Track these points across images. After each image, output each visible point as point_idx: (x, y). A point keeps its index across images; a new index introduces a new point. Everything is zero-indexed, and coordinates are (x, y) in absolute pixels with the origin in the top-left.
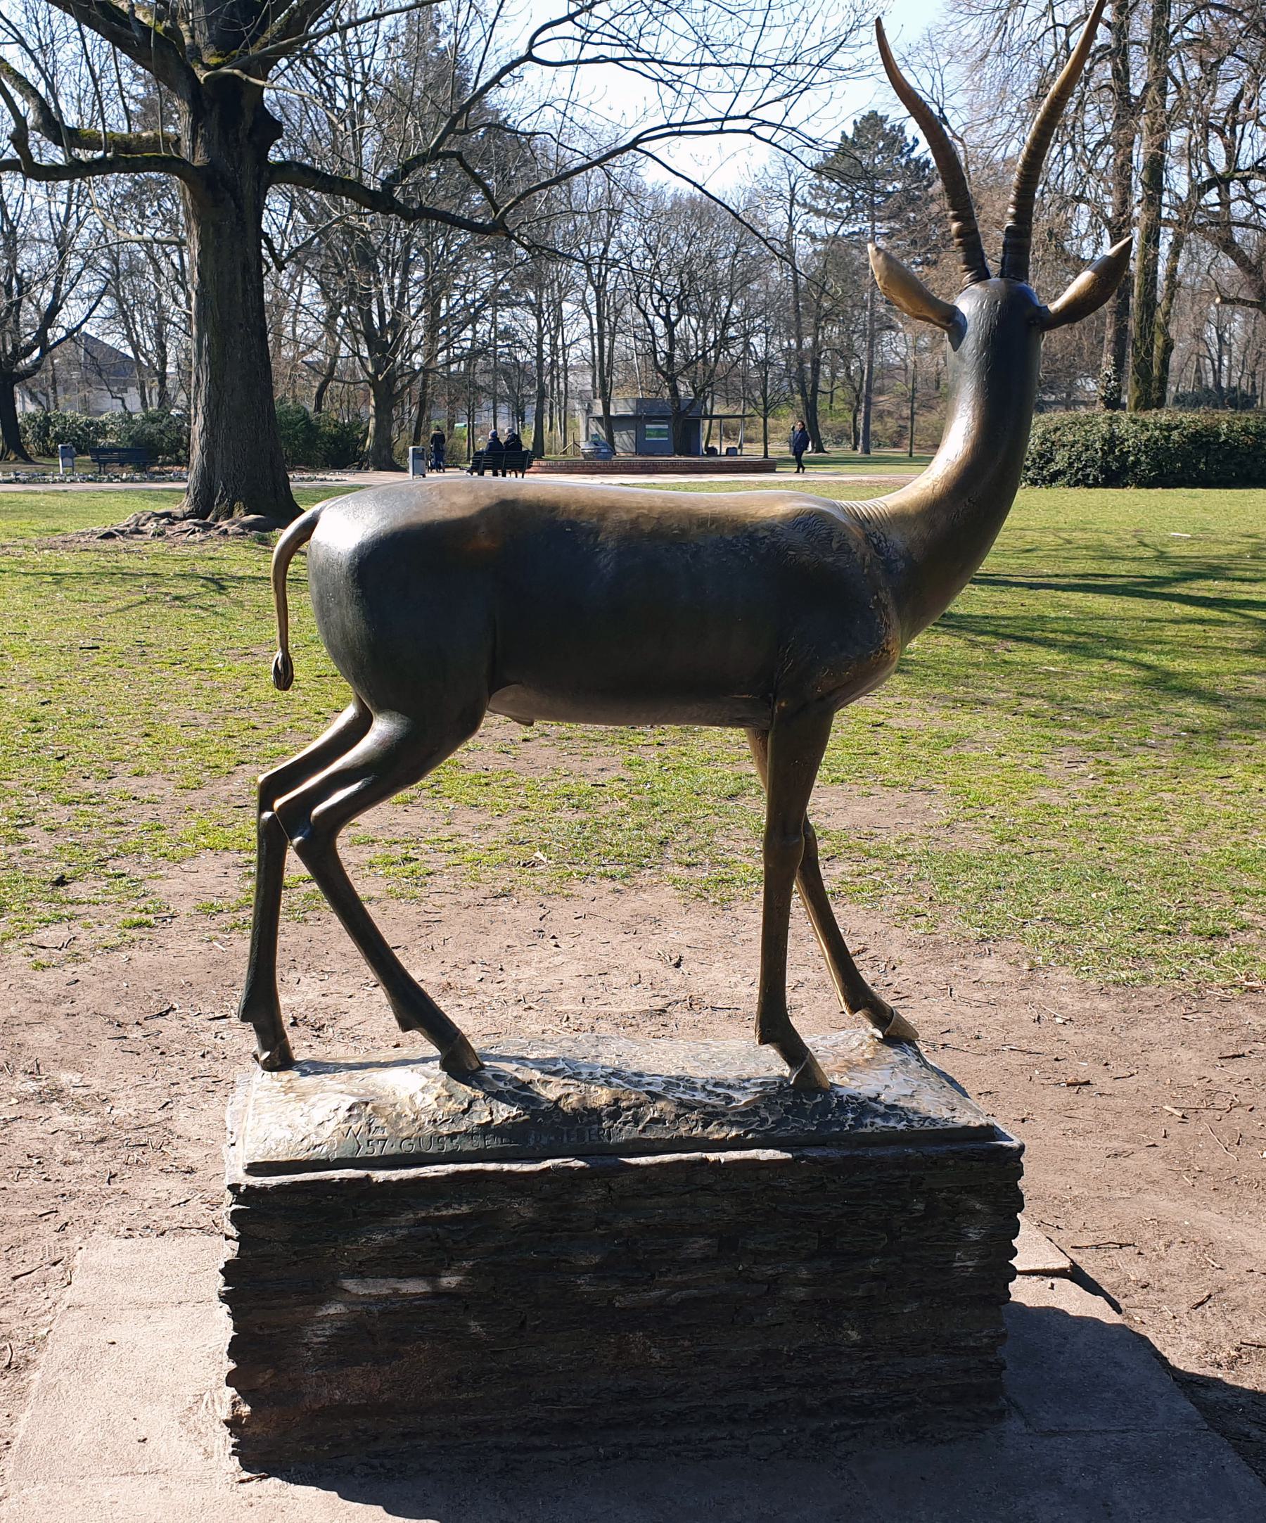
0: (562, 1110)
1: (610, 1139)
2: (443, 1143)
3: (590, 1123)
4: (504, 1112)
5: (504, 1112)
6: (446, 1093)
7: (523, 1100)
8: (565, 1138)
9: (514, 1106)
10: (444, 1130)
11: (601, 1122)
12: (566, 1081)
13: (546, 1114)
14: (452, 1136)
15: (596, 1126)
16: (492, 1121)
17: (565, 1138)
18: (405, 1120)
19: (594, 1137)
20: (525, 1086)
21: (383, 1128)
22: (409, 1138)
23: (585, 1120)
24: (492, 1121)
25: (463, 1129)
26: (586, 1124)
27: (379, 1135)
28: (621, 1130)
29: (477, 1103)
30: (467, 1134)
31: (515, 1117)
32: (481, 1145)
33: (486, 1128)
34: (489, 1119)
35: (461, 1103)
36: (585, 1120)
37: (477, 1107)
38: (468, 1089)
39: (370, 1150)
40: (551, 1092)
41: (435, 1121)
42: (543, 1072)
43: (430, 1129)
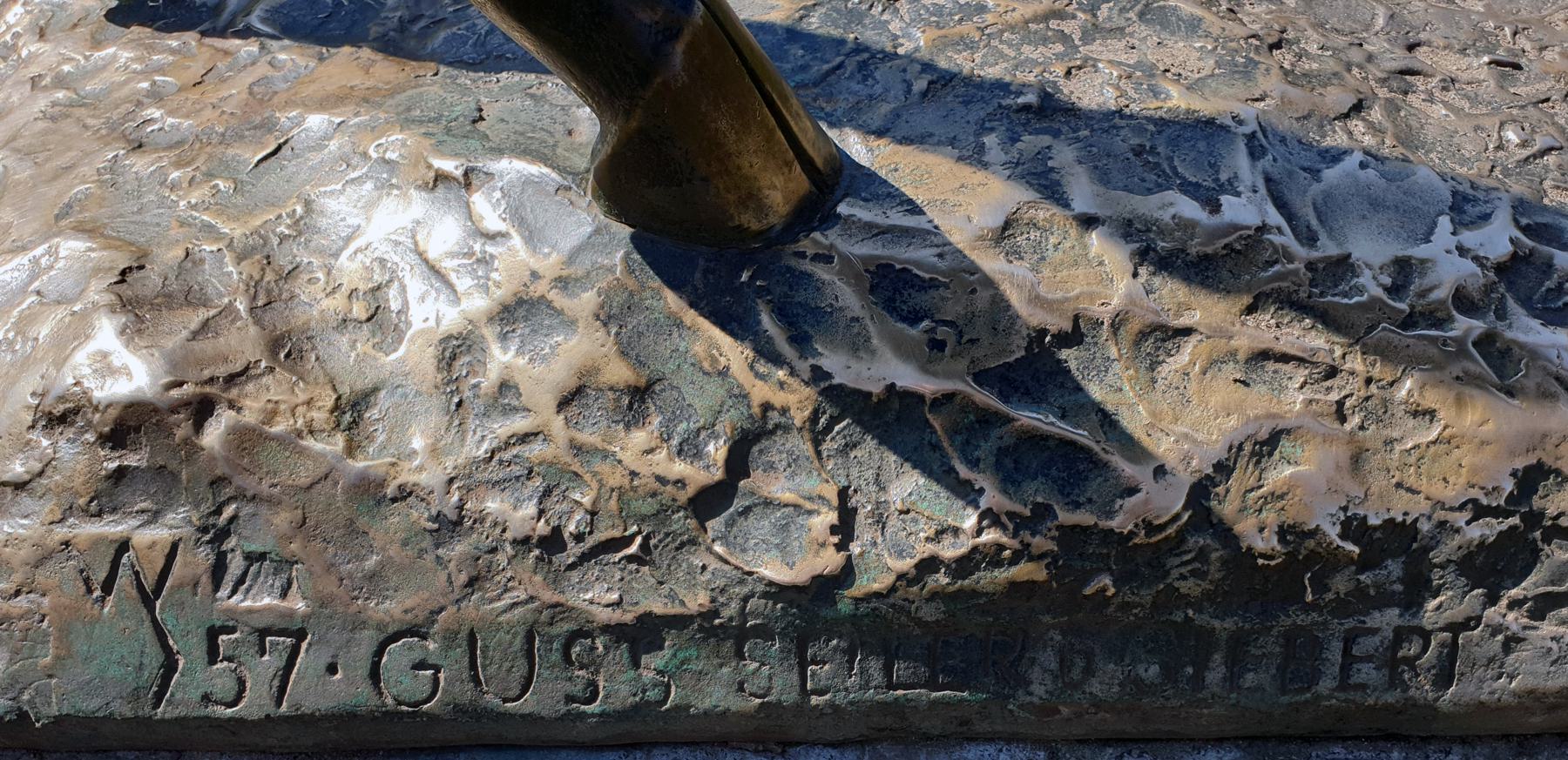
0: (1225, 534)
1: (1444, 677)
2: (593, 664)
3: (1365, 601)
4: (920, 522)
5: (920, 522)
6: (619, 372)
7: (1022, 459)
8: (1215, 674)
9: (966, 492)
10: (596, 596)
11: (1417, 589)
12: (1265, 330)
13: (1143, 556)
14: (641, 635)
15: (1389, 618)
16: (847, 573)
17: (1215, 674)
18: (396, 520)
19: (1366, 673)
20: (1039, 367)
21: (285, 564)
22: (415, 631)
23: (1340, 584)
24: (847, 573)
25: (697, 601)
26: (1342, 607)
27: (262, 600)
28: (1512, 642)
29: (777, 450)
30: (718, 632)
31: (965, 565)
32: (784, 688)
33: (810, 609)
34: (830, 561)
35: (689, 449)
36: (1340, 584)
37: (774, 482)
38: (734, 353)
39: (219, 678)
40: (1195, 403)
41: (553, 542)
42: (1158, 252)
43: (521, 588)
